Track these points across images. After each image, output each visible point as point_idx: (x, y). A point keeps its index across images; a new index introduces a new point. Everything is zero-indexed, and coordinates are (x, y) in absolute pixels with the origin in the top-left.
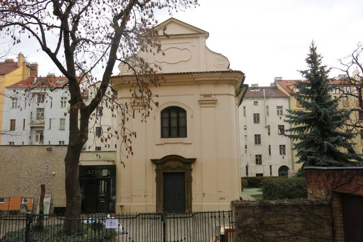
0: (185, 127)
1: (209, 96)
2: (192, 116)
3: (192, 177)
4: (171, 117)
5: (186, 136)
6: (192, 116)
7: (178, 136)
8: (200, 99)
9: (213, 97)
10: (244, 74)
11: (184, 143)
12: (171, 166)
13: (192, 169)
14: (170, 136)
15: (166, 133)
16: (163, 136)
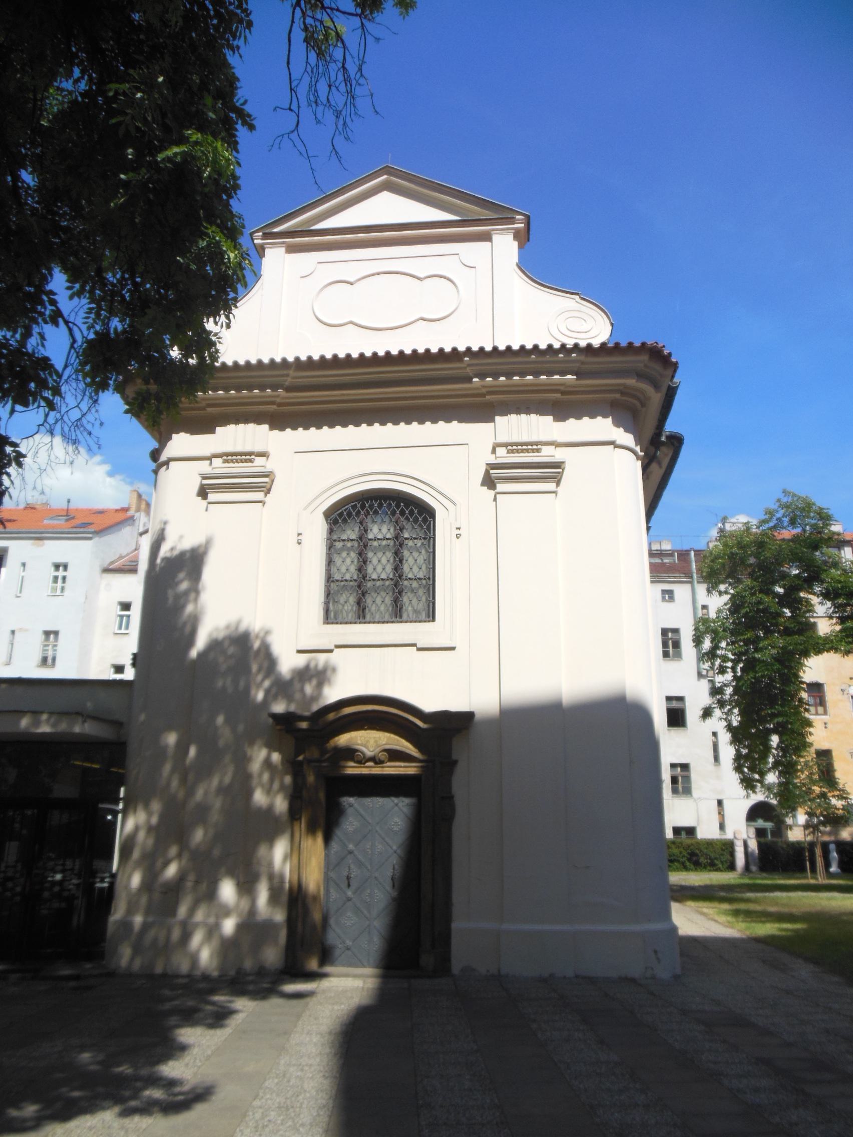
0: (429, 584)
1: (534, 446)
2: (458, 532)
3: (451, 798)
4: (371, 536)
5: (431, 616)
6: (458, 532)
7: (397, 614)
8: (492, 459)
9: (548, 454)
10: (675, 366)
11: (418, 646)
12: (362, 745)
13: (455, 763)
14: (361, 615)
15: (348, 601)
16: (330, 617)
